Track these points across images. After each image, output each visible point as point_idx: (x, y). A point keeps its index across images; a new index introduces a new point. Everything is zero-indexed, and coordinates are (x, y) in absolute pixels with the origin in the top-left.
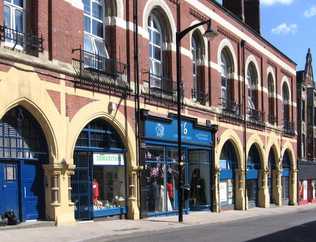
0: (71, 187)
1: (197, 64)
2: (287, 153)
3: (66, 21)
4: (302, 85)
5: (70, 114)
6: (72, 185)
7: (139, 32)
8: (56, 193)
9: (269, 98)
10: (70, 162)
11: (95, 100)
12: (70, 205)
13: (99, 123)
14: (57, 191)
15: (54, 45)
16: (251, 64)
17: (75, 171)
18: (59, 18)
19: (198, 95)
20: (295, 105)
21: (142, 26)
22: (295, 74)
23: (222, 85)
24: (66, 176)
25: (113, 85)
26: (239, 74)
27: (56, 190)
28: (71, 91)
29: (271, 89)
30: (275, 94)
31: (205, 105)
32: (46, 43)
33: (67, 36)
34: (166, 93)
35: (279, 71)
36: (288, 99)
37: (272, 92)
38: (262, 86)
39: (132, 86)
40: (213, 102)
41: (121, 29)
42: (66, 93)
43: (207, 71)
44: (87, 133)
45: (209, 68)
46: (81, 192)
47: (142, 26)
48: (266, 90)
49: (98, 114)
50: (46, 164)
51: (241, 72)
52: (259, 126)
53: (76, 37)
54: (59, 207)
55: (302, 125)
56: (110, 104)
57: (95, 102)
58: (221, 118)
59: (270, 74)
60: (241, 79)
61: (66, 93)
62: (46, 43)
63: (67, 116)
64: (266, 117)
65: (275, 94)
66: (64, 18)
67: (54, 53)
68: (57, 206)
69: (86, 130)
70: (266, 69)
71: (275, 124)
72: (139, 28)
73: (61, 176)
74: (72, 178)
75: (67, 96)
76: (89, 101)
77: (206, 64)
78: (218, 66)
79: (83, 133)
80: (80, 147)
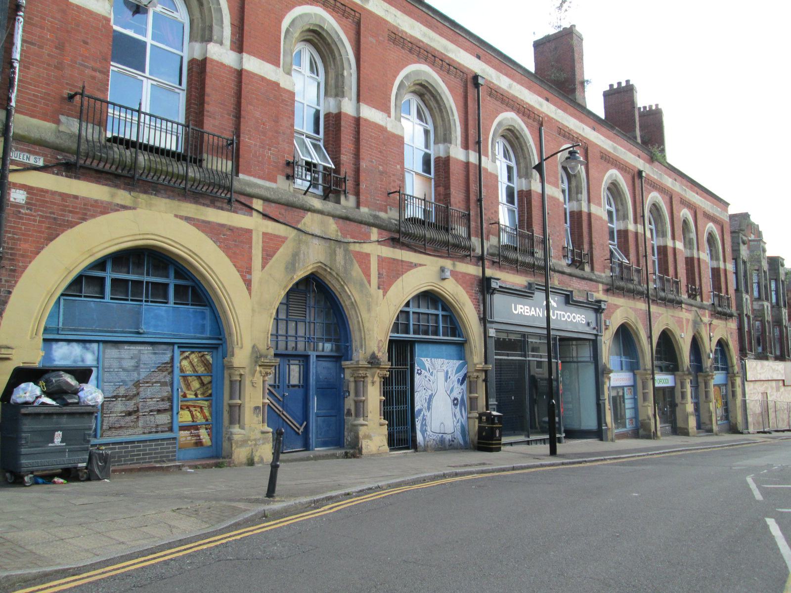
0: (384, 396)
1: (570, 208)
2: (722, 345)
3: (380, 152)
4: (741, 235)
5: (384, 285)
6: (385, 394)
7: (483, 165)
8: (361, 404)
9: (687, 258)
10: (383, 356)
11: (421, 265)
12: (381, 425)
13: (430, 297)
14: (363, 402)
15: (363, 186)
16: (655, 207)
17: (389, 371)
18: (369, 148)
19: (573, 255)
20: (730, 267)
21: (487, 156)
22: (727, 220)
23: (610, 239)
24: (377, 379)
25: (446, 244)
26: (636, 222)
27: (361, 401)
28: (388, 252)
29: (688, 243)
30: (695, 251)
31: (583, 269)
32: (350, 184)
33: (381, 173)
34: (524, 252)
35: (699, 216)
36: (718, 259)
37: (690, 249)
38: (673, 238)
39: (475, 241)
40: (596, 266)
41: (457, 160)
42: (378, 256)
43: (585, 218)
44: (408, 313)
45: (589, 215)
46: (398, 403)
47: (487, 156)
48: (679, 245)
49: (425, 285)
50: (347, 360)
51: (639, 218)
52: (671, 301)
53: (394, 175)
54: (365, 427)
55: (744, 300)
56: (442, 270)
57: (420, 268)
58: (611, 289)
59: (685, 222)
60: (640, 229)
61: (378, 256)
62: (350, 184)
63: (379, 288)
64: (683, 289)
65: (695, 251)
66: (377, 147)
67: (362, 198)
68: (363, 425)
69: (407, 309)
70: (679, 212)
71: (698, 298)
72: (483, 158)
73: (369, 380)
74: (386, 382)
75: (381, 260)
76: (412, 266)
77: (585, 209)
78: (600, 211)
79: (404, 313)
80: (396, 335)
